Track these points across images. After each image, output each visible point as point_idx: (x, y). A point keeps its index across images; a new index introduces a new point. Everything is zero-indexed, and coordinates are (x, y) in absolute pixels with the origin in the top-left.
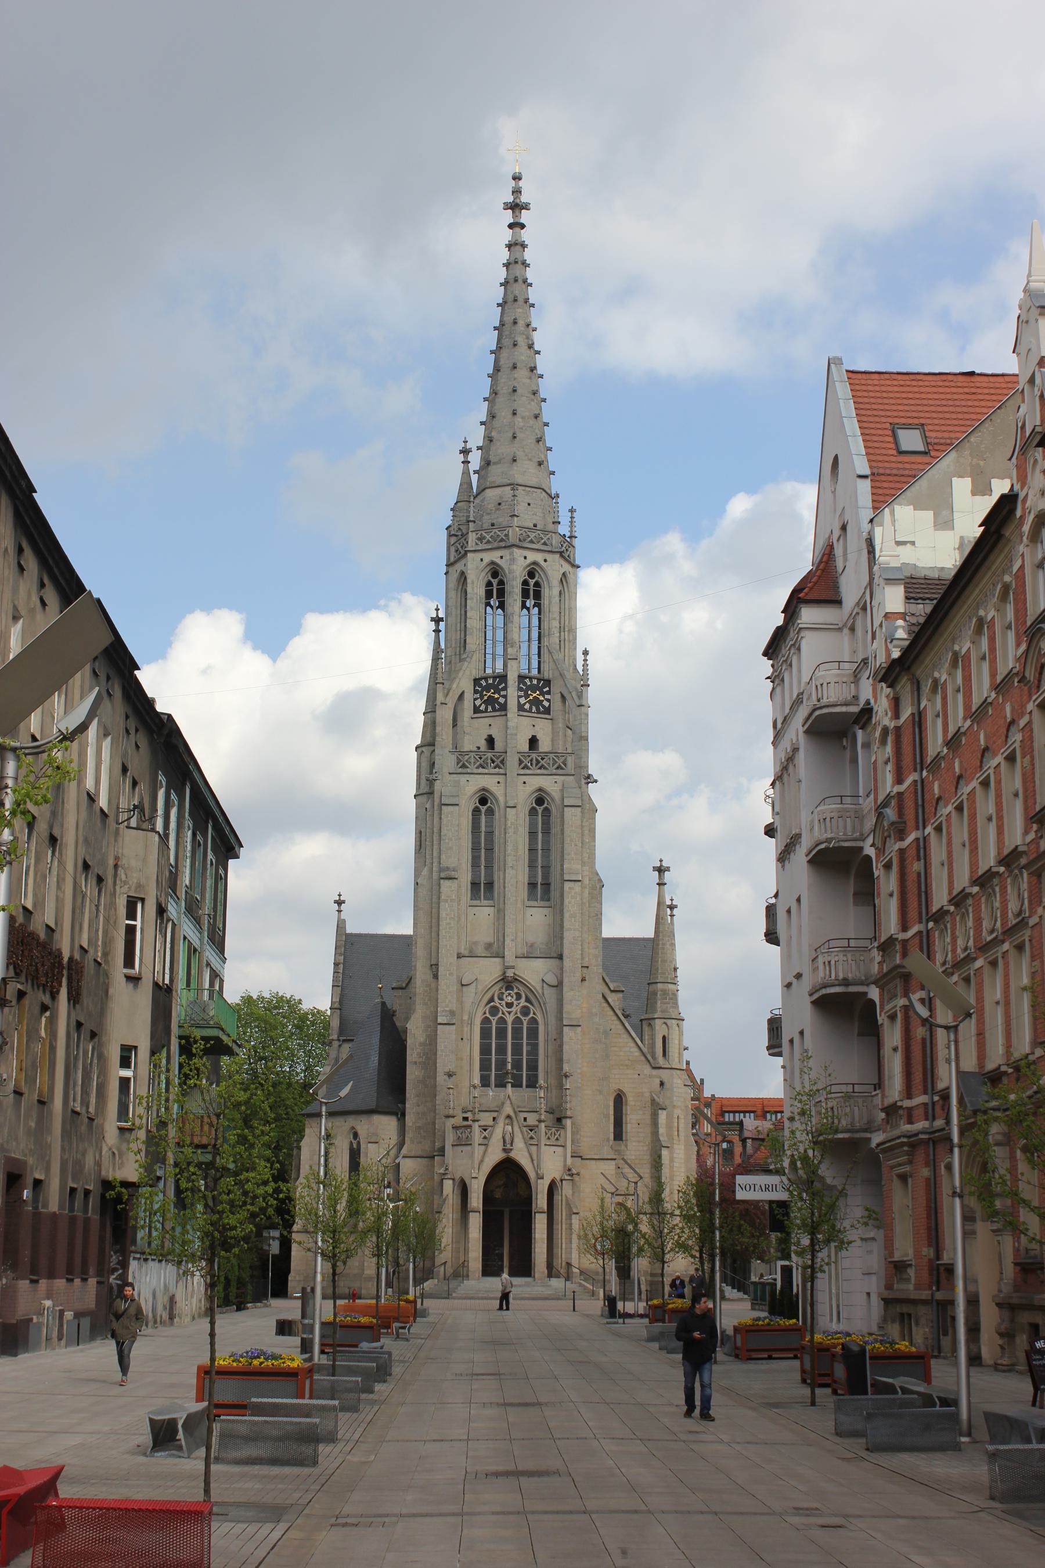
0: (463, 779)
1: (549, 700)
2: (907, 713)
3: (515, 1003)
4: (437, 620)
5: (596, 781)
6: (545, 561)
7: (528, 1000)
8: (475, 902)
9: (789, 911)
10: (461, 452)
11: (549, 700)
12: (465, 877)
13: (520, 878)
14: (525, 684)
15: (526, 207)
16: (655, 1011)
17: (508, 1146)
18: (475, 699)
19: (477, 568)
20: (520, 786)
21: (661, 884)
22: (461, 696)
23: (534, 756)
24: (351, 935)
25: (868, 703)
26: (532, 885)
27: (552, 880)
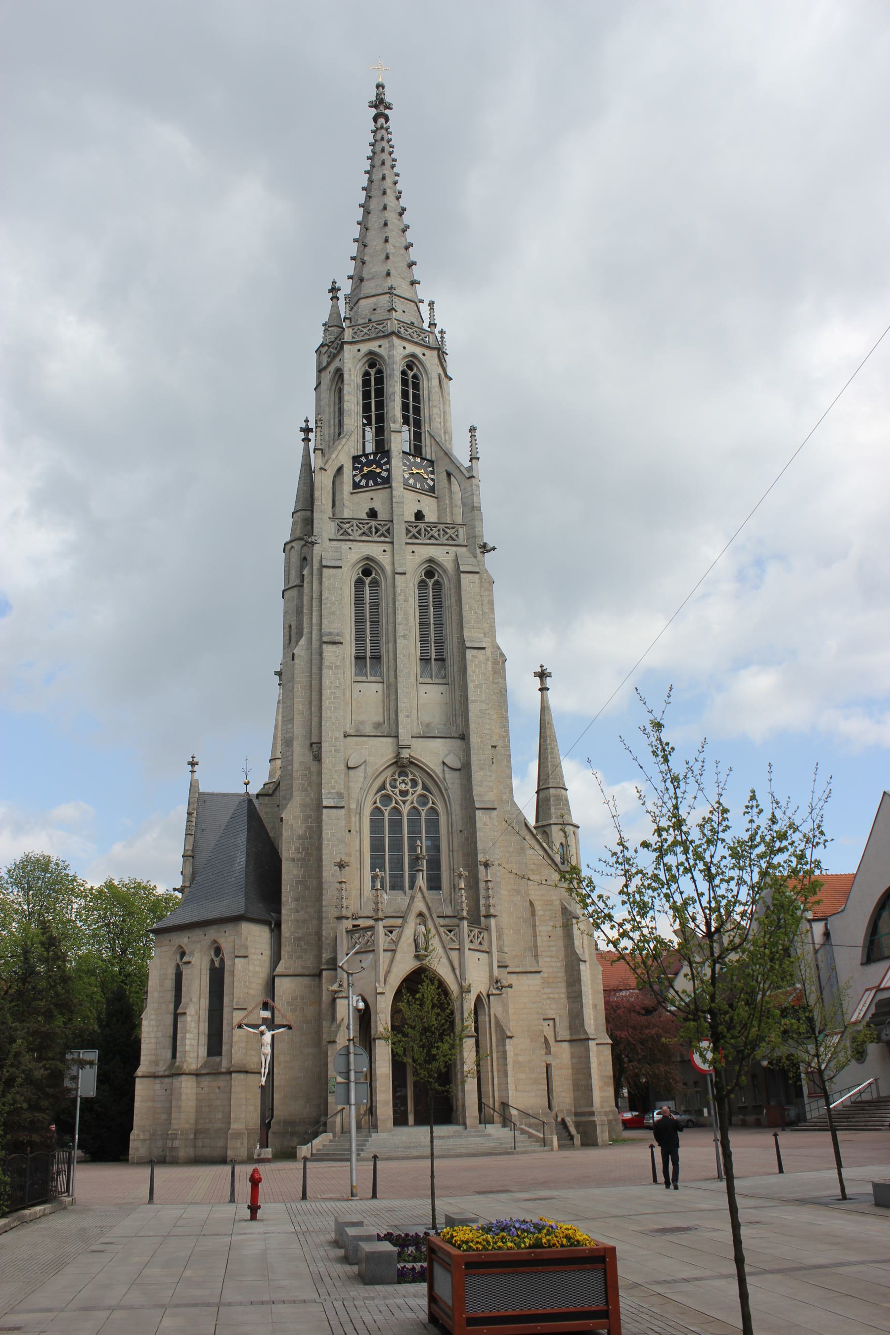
0: (345, 546)
3: (411, 790)
4: (307, 430)
5: (494, 549)
6: (424, 355)
7: (425, 787)
10: (330, 291)
11: (433, 480)
12: (349, 649)
13: (413, 651)
14: (409, 460)
15: (389, 107)
16: (550, 818)
17: (422, 952)
19: (354, 357)
20: (409, 556)
21: (543, 689)
22: (340, 469)
24: (204, 794)
26: (425, 660)
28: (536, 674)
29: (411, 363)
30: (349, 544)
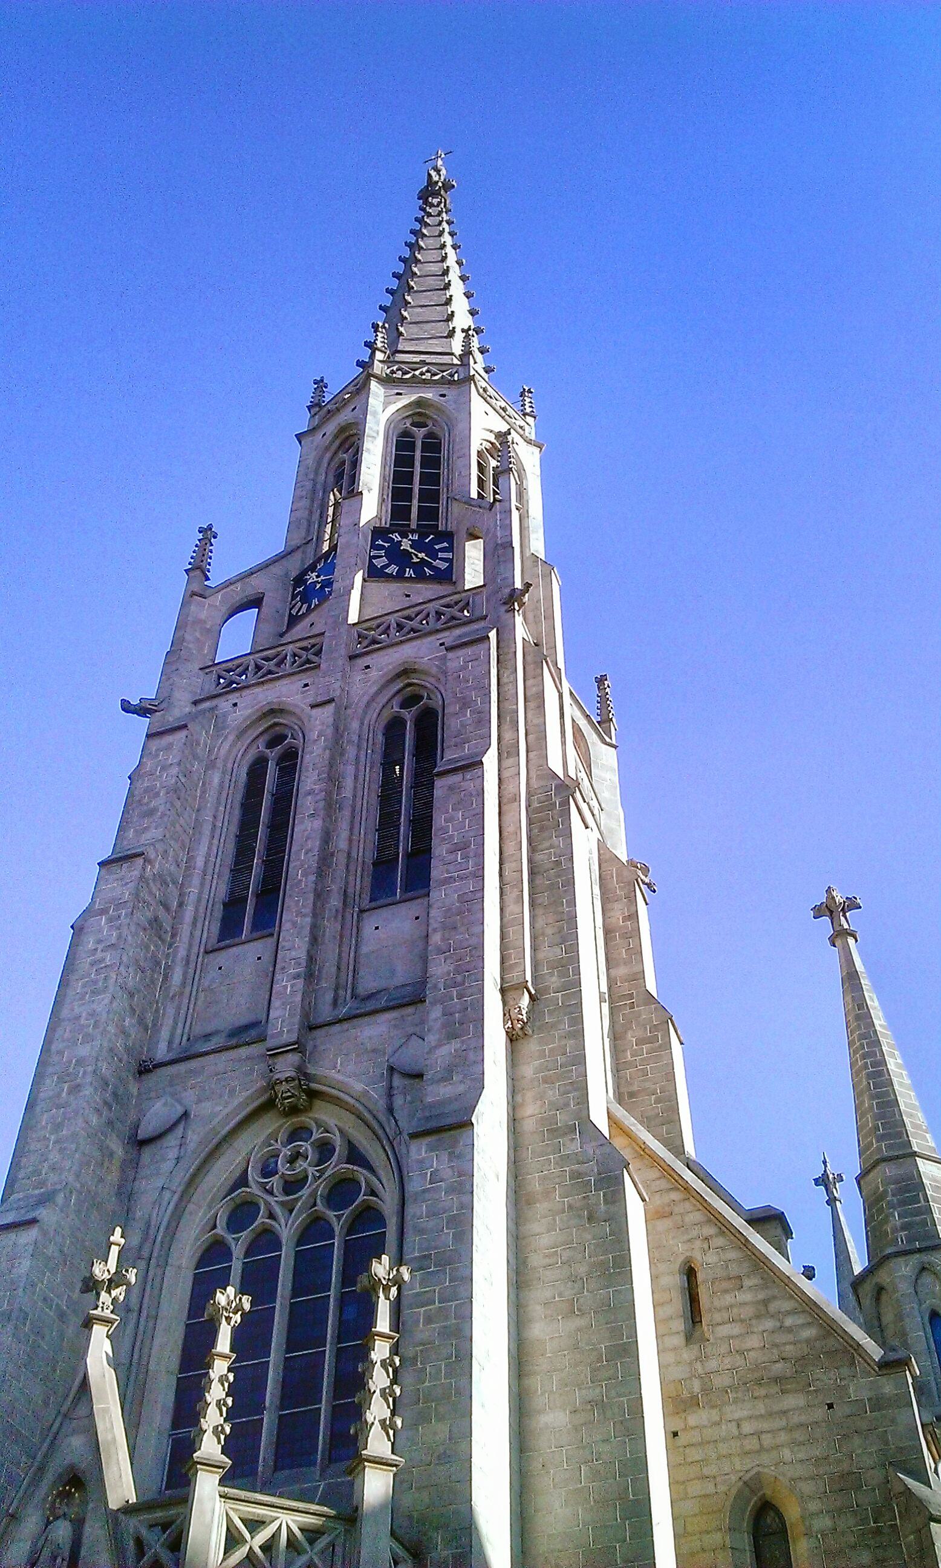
30: (233, 698)
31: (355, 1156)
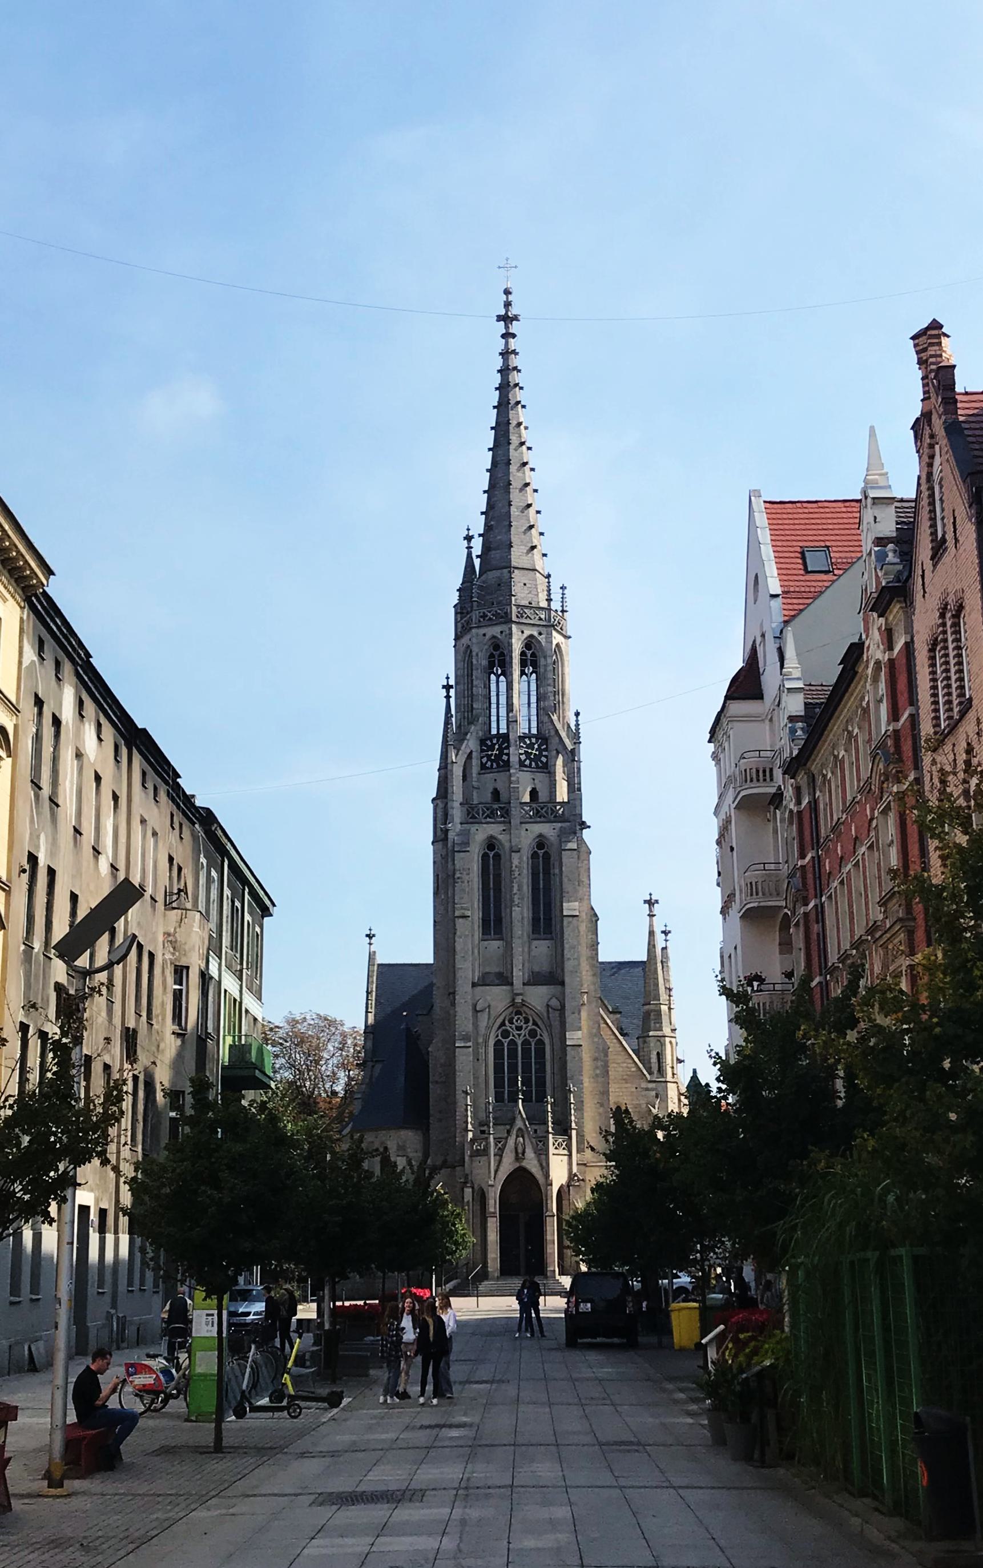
0: (473, 828)
1: (546, 756)
2: (805, 801)
3: (524, 1026)
4: (447, 687)
6: (540, 634)
7: (535, 1023)
8: (486, 937)
9: (730, 957)
10: (465, 538)
11: (546, 756)
12: (476, 914)
14: (525, 743)
18: (482, 758)
20: (523, 832)
22: (470, 756)
23: (534, 805)
25: (779, 788)
26: (535, 921)
27: (553, 916)
28: (645, 902)
29: (529, 643)
30: (476, 826)
31: (535, 1023)
